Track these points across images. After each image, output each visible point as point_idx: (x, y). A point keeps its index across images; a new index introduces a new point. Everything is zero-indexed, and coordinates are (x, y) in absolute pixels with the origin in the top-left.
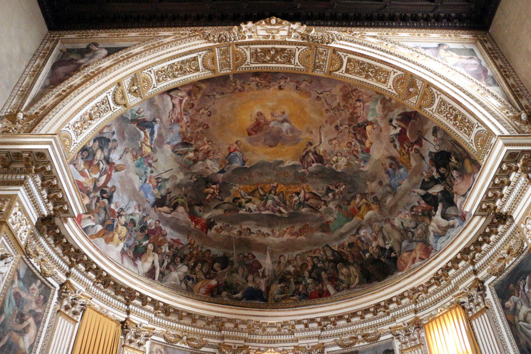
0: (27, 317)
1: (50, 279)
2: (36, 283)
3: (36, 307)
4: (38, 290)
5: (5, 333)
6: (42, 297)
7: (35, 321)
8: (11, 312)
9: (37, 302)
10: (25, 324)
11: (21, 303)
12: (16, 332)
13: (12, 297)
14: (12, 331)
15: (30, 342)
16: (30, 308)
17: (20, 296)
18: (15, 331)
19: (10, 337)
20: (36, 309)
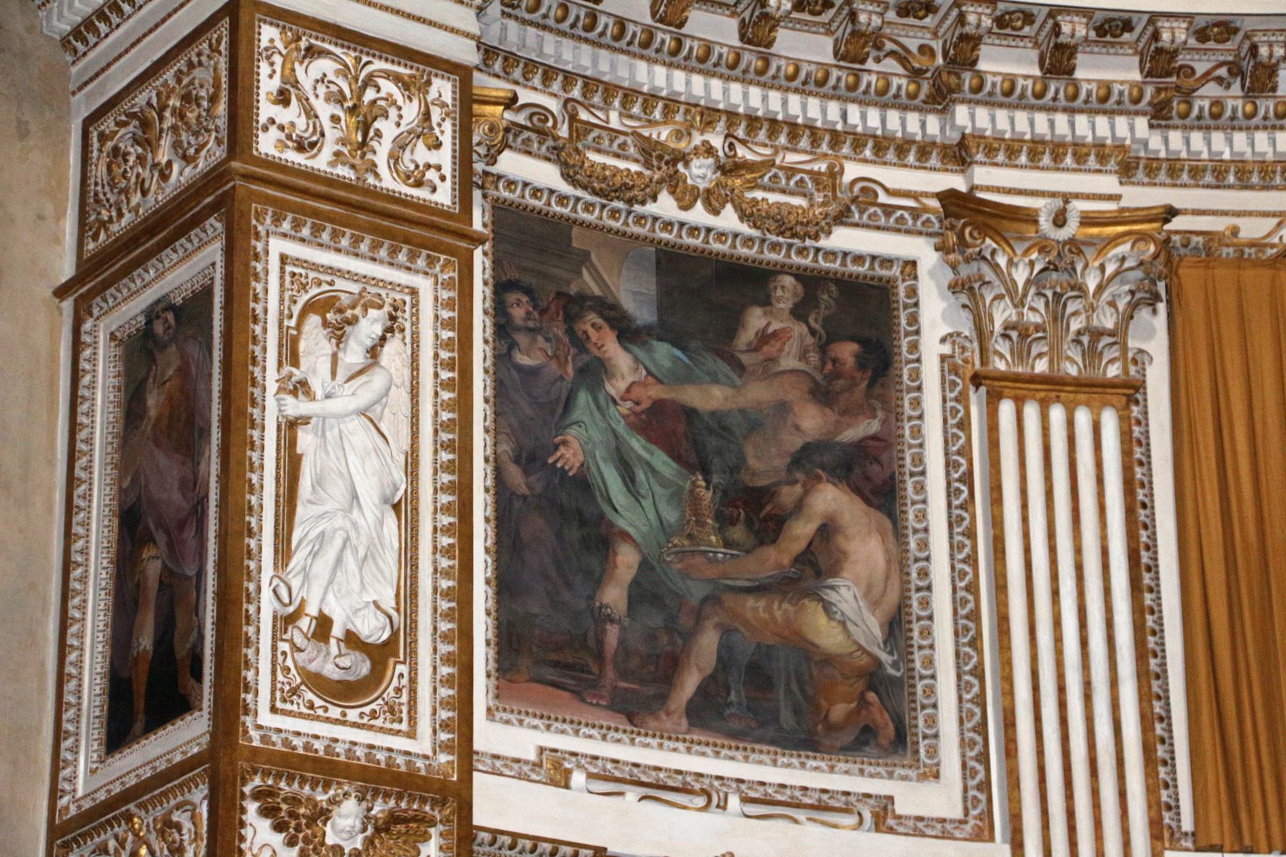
0: (788, 495)
1: (843, 239)
2: (766, 302)
3: (832, 416)
4: (799, 329)
5: (685, 621)
6: (847, 351)
7: (857, 491)
8: (671, 515)
9: (823, 394)
10: (802, 531)
11: (712, 443)
12: (759, 589)
13: (637, 444)
14: (729, 600)
15: (874, 605)
16: (794, 443)
17: (690, 413)
18: (748, 590)
19: (726, 632)
20: (838, 428)
